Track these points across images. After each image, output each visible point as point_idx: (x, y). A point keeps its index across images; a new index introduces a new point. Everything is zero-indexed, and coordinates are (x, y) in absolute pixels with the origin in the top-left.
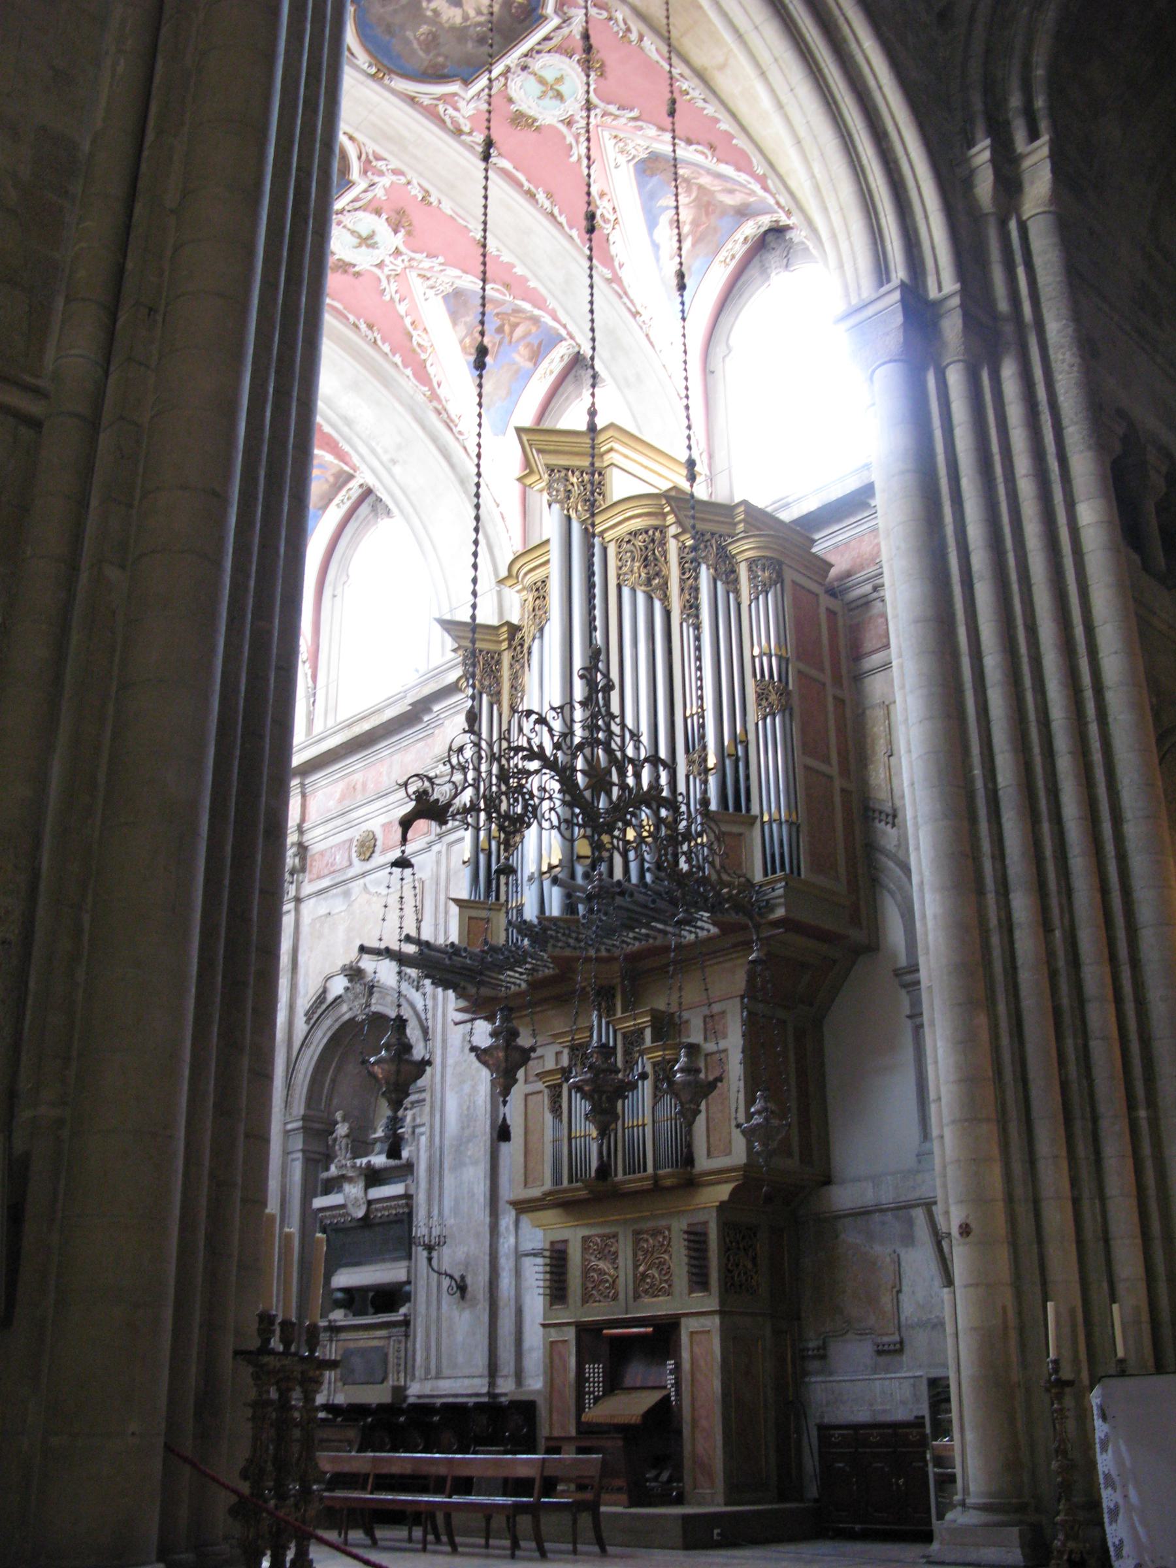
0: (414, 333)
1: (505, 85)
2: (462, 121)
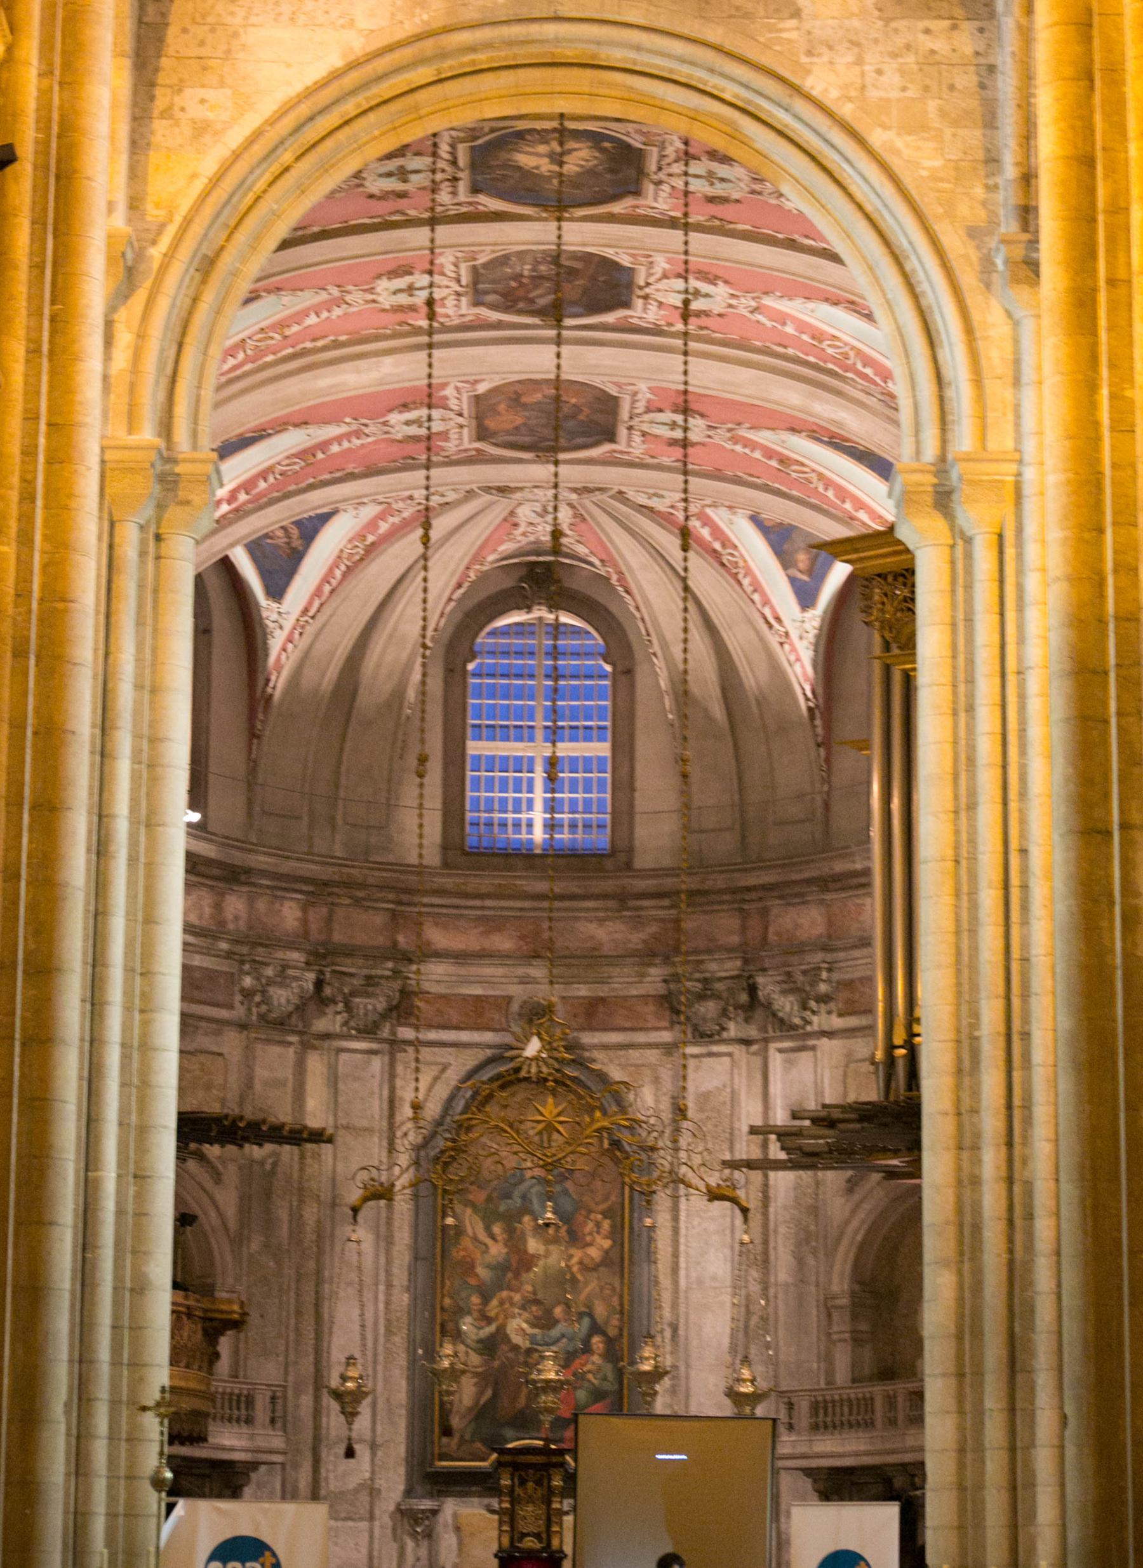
0: (824, 345)
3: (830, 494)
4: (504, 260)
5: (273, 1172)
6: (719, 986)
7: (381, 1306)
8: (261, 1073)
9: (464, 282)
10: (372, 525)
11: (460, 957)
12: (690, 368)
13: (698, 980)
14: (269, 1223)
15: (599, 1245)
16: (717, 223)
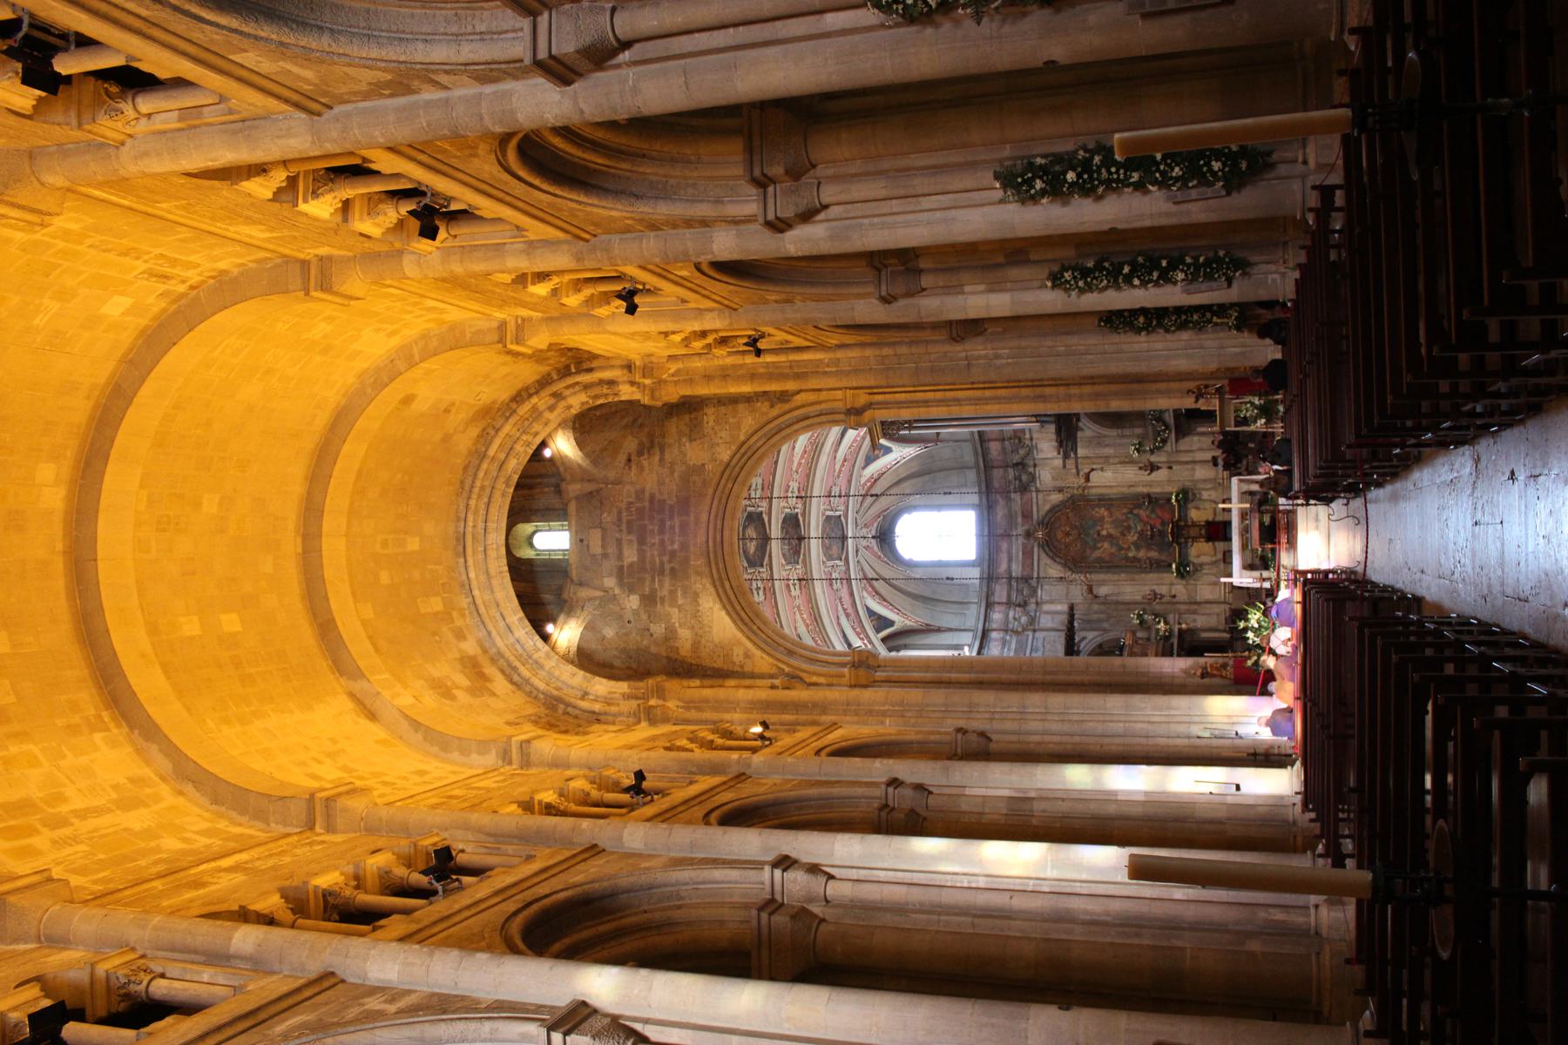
4: (784, 555)
5: (1083, 620)
8: (1050, 625)
10: (869, 593)
11: (1010, 560)
14: (1099, 621)
15: (1103, 512)
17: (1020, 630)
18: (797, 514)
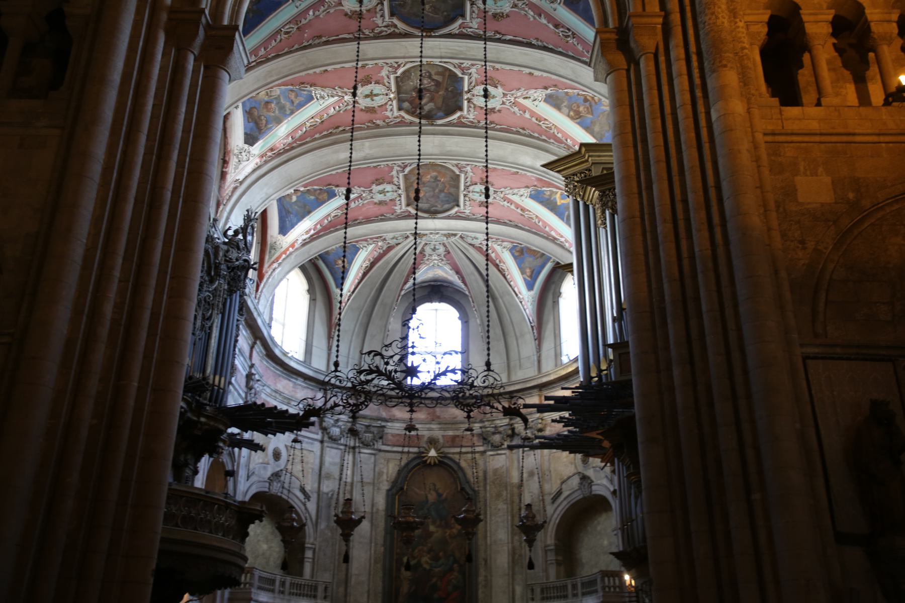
0: (541, 123)
1: (478, 7)
2: (477, 31)
3: (540, 224)
5: (331, 498)
6: (501, 429)
7: (373, 552)
8: (328, 459)
9: (393, 91)
12: (488, 143)
13: (492, 427)
16: (498, 36)
17: (324, 424)
18: (461, 109)
